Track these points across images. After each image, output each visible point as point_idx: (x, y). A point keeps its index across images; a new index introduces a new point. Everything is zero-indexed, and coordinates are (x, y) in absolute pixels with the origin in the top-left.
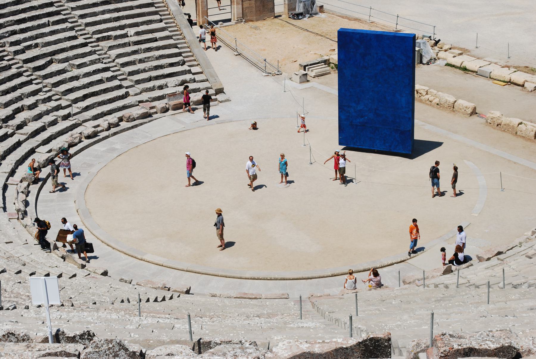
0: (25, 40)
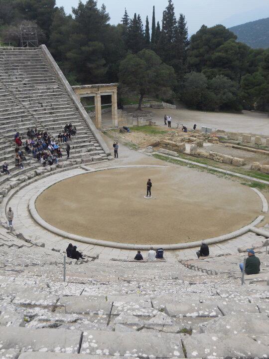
0: (9, 127)
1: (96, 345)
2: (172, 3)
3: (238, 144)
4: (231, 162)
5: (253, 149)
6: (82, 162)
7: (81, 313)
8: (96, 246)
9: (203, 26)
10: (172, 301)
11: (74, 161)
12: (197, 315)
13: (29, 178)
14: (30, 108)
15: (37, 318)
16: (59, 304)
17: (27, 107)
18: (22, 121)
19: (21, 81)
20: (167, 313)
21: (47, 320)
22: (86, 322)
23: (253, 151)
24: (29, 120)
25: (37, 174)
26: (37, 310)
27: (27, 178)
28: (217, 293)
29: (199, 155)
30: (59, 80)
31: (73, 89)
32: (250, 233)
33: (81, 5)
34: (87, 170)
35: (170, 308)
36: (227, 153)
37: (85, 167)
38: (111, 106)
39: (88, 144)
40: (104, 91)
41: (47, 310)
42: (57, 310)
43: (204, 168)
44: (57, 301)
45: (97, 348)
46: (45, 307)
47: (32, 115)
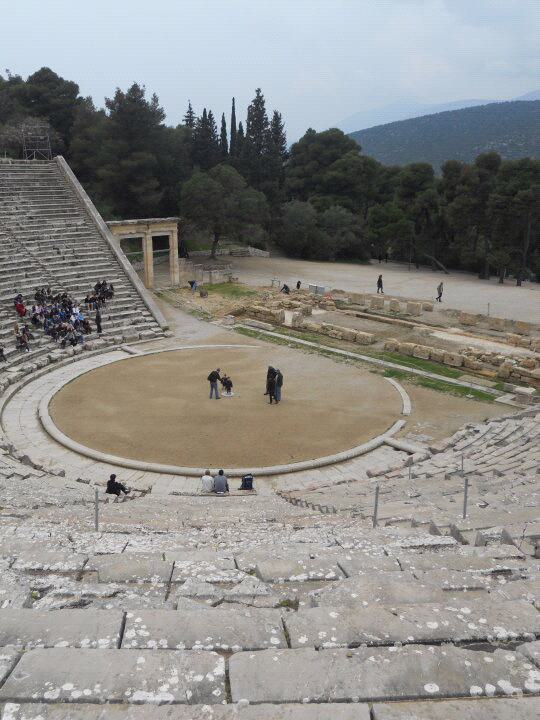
1: (147, 634)
2: (261, 94)
3: (365, 311)
4: (355, 339)
5: (387, 319)
6: (124, 340)
7: (123, 582)
9: (310, 130)
10: (266, 558)
12: (306, 577)
13: (39, 367)
14: (39, 255)
15: (52, 593)
16: (87, 567)
17: (34, 253)
18: (27, 276)
19: (24, 213)
20: (259, 576)
21: (68, 596)
22: (132, 596)
23: (386, 322)
24: (39, 275)
25: (52, 361)
26: (52, 578)
27: (35, 366)
28: (337, 542)
29: (306, 329)
30: (87, 212)
31: (108, 226)
32: (385, 447)
33: (119, 95)
34: (131, 353)
35: (265, 568)
36: (349, 325)
37: (128, 349)
38: (168, 253)
39: (133, 312)
40: (157, 229)
41: (67, 578)
42: (85, 577)
43: (314, 348)
44: (85, 562)
45: (149, 638)
46: (66, 574)
47: (43, 267)
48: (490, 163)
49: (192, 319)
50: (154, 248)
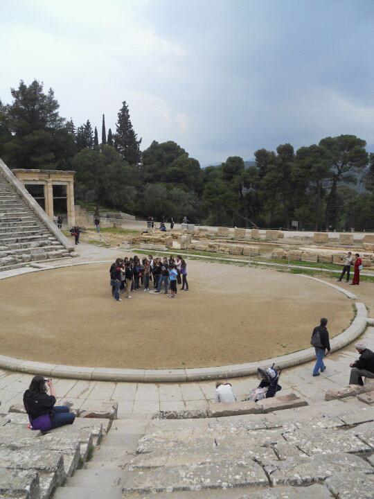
2: (126, 105)
3: (232, 239)
8: (93, 383)
9: (154, 142)
11: (19, 258)
33: (22, 87)
34: (39, 268)
37: (37, 265)
39: (40, 236)
40: (57, 179)
48: (286, 150)
49: (91, 246)
50: (54, 195)
